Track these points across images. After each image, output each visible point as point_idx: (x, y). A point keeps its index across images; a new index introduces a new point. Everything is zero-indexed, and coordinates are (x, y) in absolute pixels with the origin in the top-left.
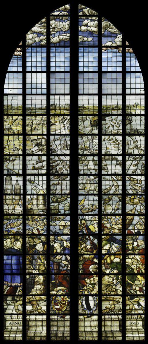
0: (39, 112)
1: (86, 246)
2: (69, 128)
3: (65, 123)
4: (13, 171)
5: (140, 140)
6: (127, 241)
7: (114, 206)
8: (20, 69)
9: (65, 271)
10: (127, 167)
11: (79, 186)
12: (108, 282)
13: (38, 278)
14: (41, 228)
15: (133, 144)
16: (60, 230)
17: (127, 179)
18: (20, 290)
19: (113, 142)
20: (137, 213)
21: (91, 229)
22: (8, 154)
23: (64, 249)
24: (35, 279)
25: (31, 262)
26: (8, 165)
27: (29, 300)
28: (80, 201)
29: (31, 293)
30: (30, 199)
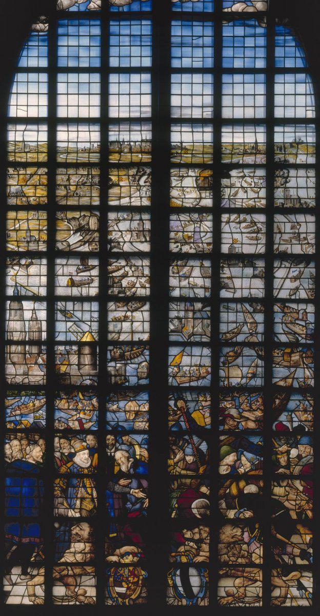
0: (83, 158)
1: (184, 457)
2: (149, 194)
3: (142, 182)
4: (27, 290)
5: (306, 222)
6: (277, 446)
7: (245, 370)
8: (44, 63)
10: (277, 283)
11: (170, 324)
12: (233, 537)
13: (78, 528)
14: (86, 417)
15: (291, 231)
16: (126, 421)
17: (276, 308)
18: (40, 553)
19: (246, 228)
20: (296, 385)
22: (16, 251)
23: (137, 463)
24: (72, 529)
25: (64, 491)
26: (16, 275)
27: (59, 573)
28: (174, 357)
29: (63, 560)
30: (63, 352)
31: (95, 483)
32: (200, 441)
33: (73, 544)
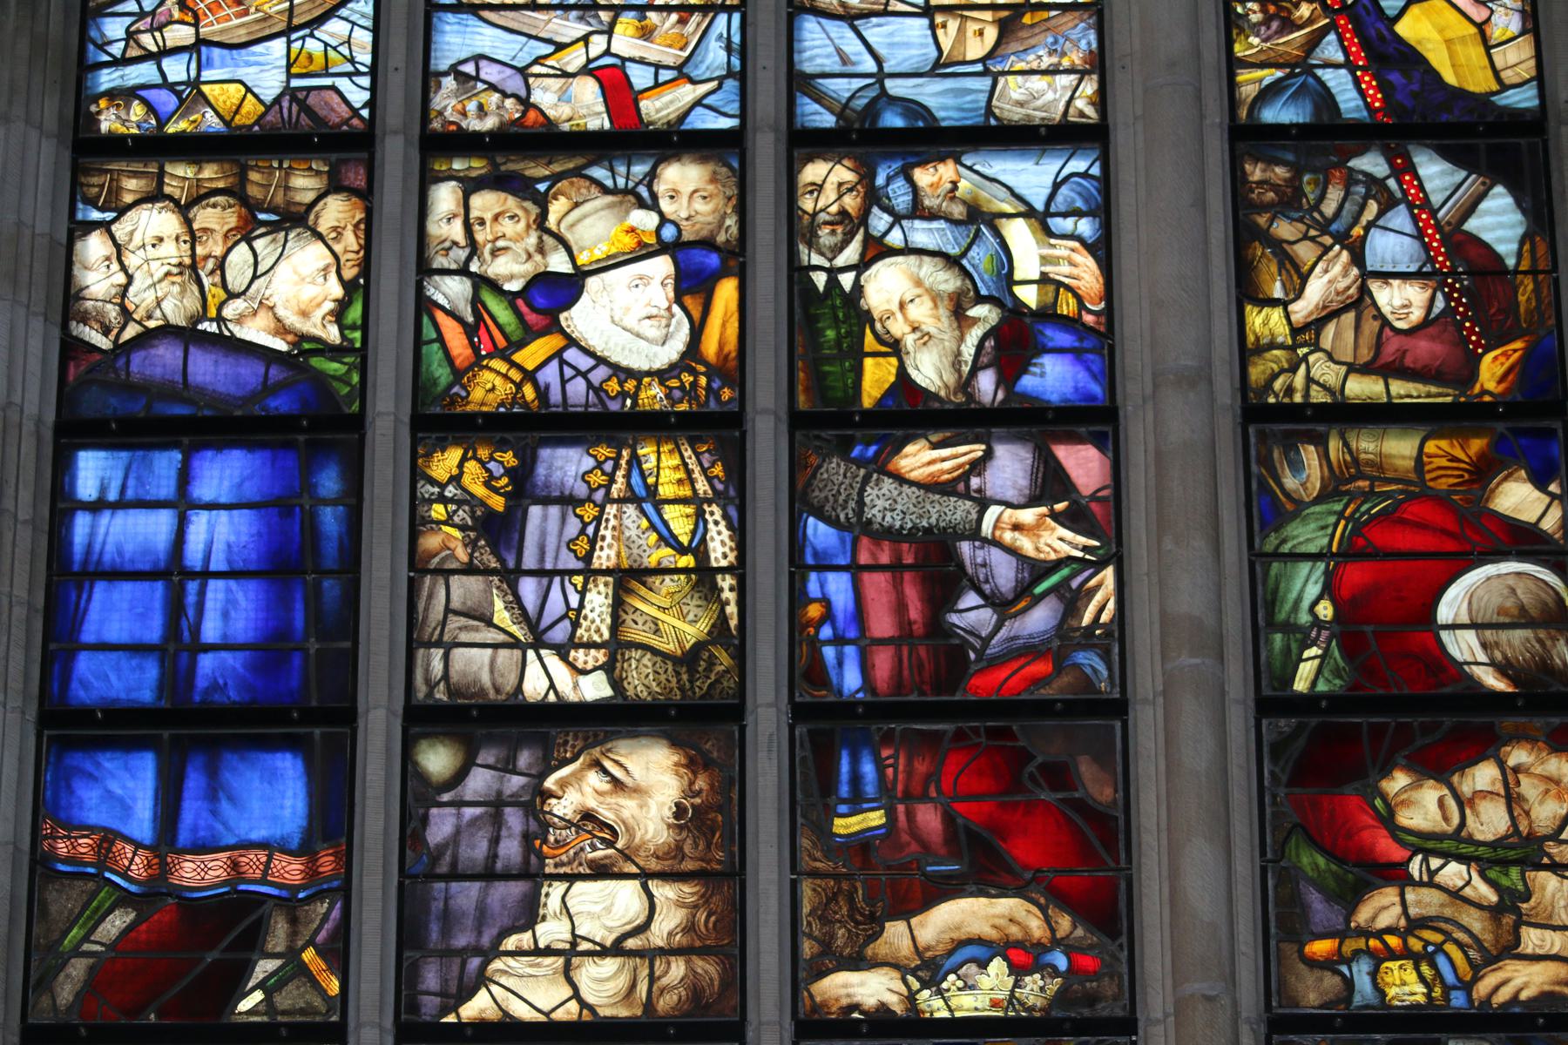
1: (1364, 291)
9: (1041, 667)
13: (594, 779)
14: (654, 52)
16: (940, 67)
18: (309, 955)
21: (1439, 59)
24: (550, 783)
31: (718, 470)
32: (1473, 183)
33: (558, 889)
